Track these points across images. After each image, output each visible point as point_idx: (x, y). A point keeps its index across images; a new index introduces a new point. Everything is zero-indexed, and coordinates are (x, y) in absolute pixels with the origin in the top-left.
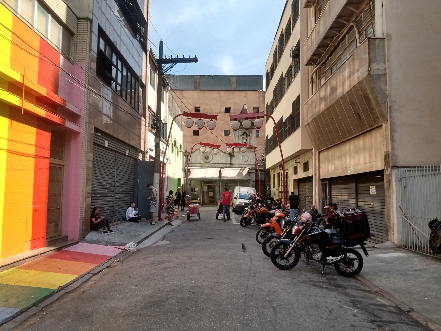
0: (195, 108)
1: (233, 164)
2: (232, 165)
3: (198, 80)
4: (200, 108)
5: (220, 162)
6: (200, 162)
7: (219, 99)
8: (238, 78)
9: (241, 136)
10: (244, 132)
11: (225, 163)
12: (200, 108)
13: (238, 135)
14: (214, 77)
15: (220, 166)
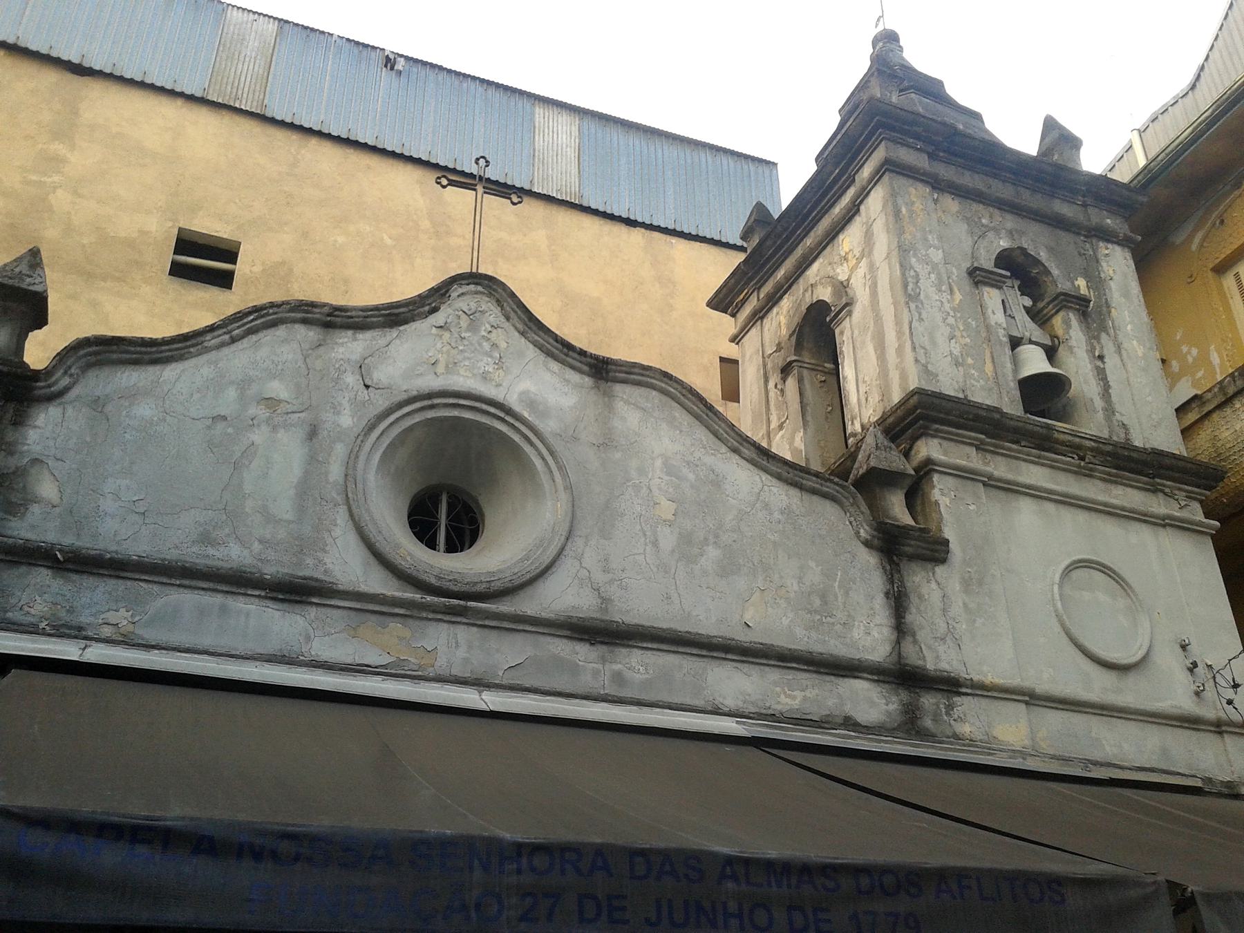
0: (187, 243)
1: (951, 686)
2: (929, 701)
3: (253, 44)
4: (229, 253)
5: (707, 622)
6: (309, 569)
7: (425, 224)
8: (592, 126)
9: (978, 277)
10: (1004, 243)
11: (802, 639)
12: (229, 253)
13: (937, 256)
14: (401, 61)
15: (730, 703)
